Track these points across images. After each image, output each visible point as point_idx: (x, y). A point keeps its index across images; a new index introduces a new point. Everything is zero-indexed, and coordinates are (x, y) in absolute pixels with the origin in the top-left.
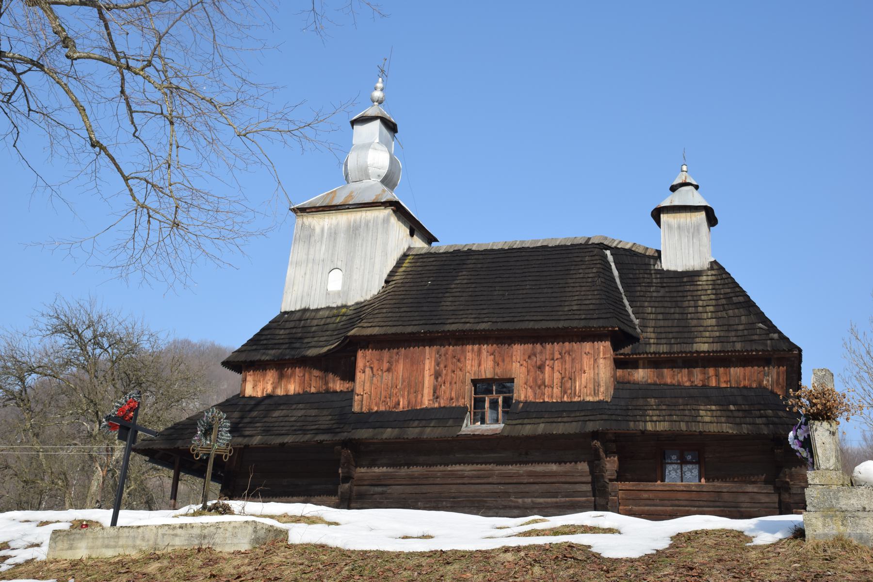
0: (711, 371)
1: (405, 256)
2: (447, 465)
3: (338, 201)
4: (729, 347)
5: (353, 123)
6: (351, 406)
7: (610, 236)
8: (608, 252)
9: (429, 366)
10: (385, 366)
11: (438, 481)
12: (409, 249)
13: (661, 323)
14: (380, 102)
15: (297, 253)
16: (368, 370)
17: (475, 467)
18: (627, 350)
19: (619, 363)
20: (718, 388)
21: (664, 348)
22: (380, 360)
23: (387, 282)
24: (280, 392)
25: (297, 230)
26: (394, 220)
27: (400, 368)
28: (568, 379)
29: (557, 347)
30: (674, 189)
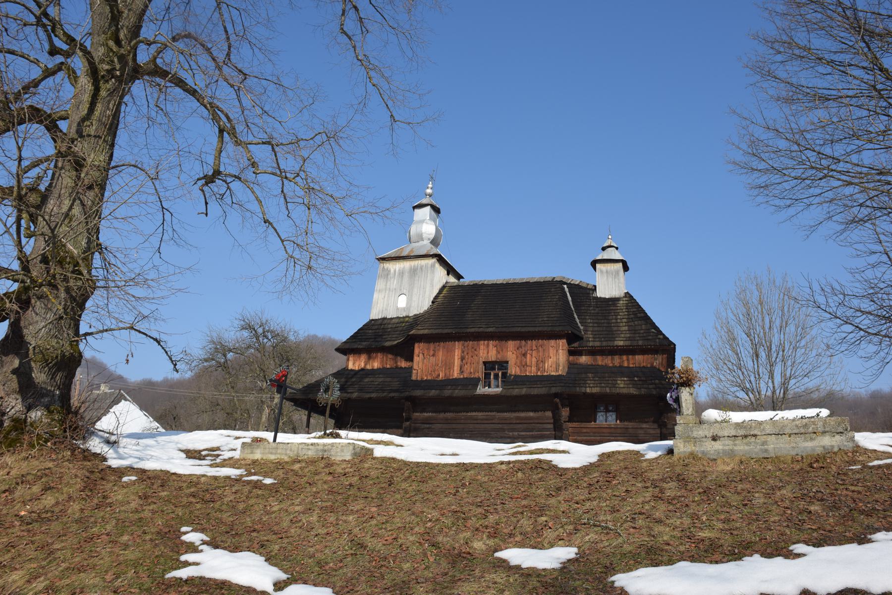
0: (625, 357)
1: (444, 287)
3: (404, 254)
4: (635, 343)
5: (414, 208)
6: (411, 376)
7: (567, 276)
8: (565, 286)
9: (457, 354)
10: (432, 353)
11: (462, 421)
12: (447, 282)
13: (596, 329)
14: (430, 196)
15: (380, 284)
16: (421, 355)
17: (484, 413)
18: (576, 345)
19: (571, 353)
20: (628, 367)
21: (597, 344)
22: (428, 349)
23: (433, 302)
24: (369, 367)
25: (380, 271)
26: (437, 265)
27: (441, 354)
28: (541, 362)
29: (534, 342)
30: (604, 249)
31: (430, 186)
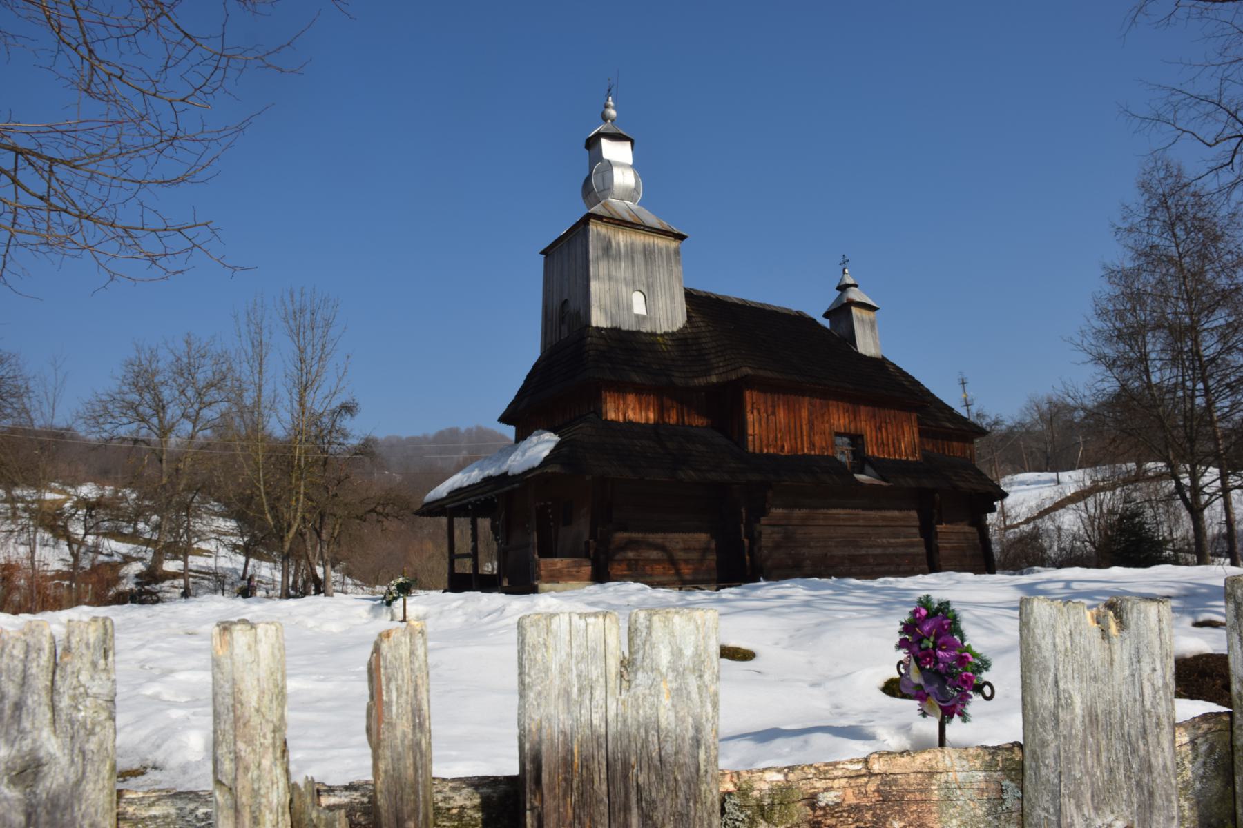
2: (828, 508)
9: (805, 413)
27: (781, 413)
31: (611, 103)
